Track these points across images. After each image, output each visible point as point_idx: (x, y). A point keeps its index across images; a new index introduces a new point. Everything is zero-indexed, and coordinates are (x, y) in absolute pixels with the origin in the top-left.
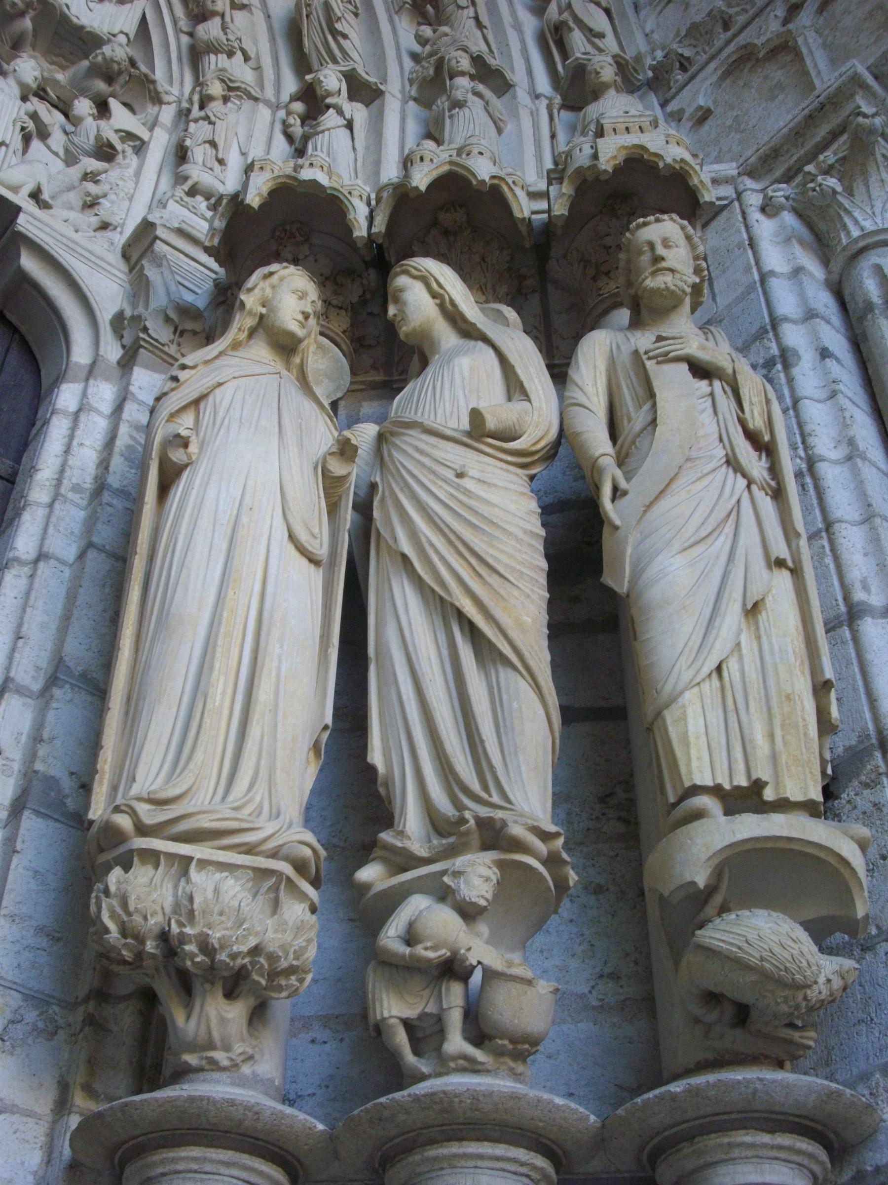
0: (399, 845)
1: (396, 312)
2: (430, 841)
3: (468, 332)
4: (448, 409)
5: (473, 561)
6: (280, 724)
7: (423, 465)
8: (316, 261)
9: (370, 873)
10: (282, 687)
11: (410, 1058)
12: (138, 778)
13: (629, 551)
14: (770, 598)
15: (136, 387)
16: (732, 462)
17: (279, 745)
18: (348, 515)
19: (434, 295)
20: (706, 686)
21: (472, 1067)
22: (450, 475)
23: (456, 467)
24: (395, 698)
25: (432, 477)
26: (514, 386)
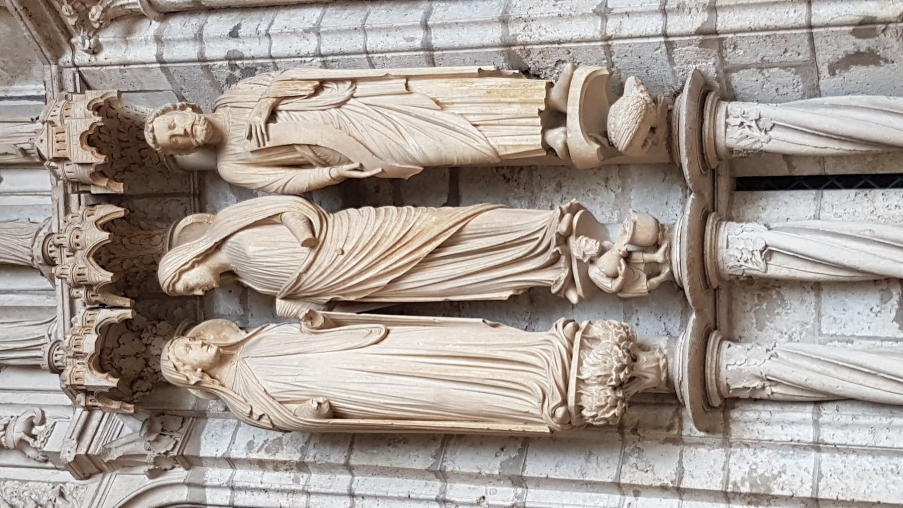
0: (562, 282)
2: (560, 268)
3: (218, 247)
5: (398, 246)
7: (332, 272)
9: (573, 297)
11: (662, 277)
12: (526, 410)
13: (397, 165)
16: (339, 106)
18: (336, 314)
19: (193, 267)
21: (669, 249)
22: (341, 258)
24: (474, 286)
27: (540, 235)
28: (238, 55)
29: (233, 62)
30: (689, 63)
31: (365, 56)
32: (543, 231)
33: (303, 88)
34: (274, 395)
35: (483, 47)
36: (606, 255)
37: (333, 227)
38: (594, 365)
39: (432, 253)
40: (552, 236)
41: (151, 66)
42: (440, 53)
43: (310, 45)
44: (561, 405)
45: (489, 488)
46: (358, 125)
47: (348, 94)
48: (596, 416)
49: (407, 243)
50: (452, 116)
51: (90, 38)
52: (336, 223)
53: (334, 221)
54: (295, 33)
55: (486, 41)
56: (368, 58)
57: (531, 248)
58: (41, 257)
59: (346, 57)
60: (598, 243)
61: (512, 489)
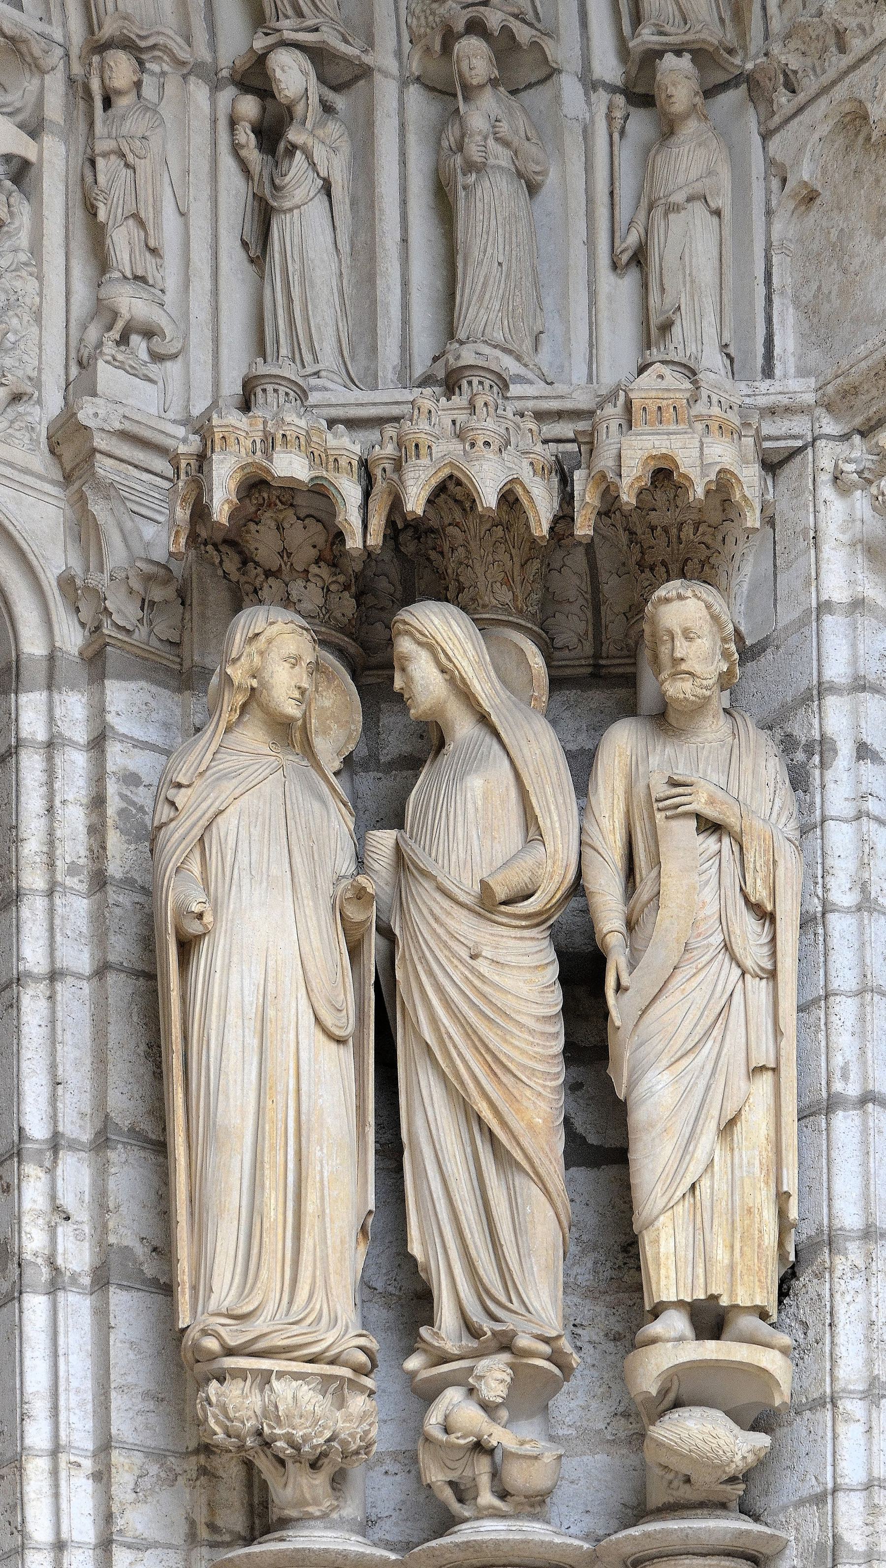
1: (403, 685)
3: (484, 719)
4: (462, 855)
5: (489, 1059)
6: (328, 1230)
8: (305, 528)
10: (326, 1192)
13: (627, 1054)
14: (747, 1108)
15: (113, 713)
16: (727, 947)
17: (330, 1250)
20: (679, 1209)
23: (471, 945)
25: (447, 953)
26: (531, 825)
27: (516, 1305)
28: (827, 760)
29: (817, 748)
30: (797, 1529)
31: (822, 992)
32: (522, 1311)
33: (759, 882)
34: (214, 828)
35: (830, 1199)
36: (482, 1413)
37: (521, 938)
38: (295, 1398)
39: (479, 1119)
40: (510, 1322)
41: (813, 589)
42: (824, 1125)
43: (842, 894)
44: (223, 1345)
45: (87, 1229)
46: (694, 982)
47: (749, 963)
48: (210, 1404)
49: (495, 1074)
50: (708, 1149)
51: (860, 473)
52: (529, 943)
53: (532, 939)
54: (863, 865)
55: (838, 1204)
56: (819, 999)
57: (493, 1291)
58: (462, 363)
59: (822, 959)
60: (500, 1400)
61: (87, 1268)
